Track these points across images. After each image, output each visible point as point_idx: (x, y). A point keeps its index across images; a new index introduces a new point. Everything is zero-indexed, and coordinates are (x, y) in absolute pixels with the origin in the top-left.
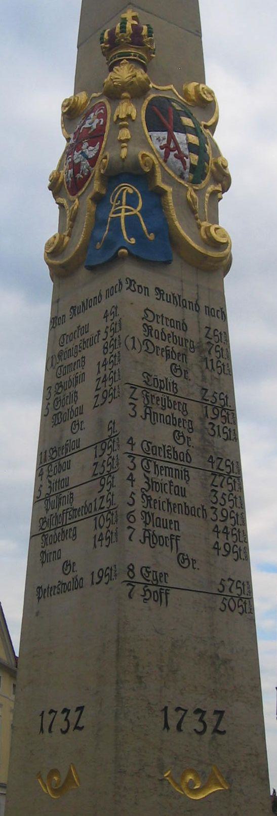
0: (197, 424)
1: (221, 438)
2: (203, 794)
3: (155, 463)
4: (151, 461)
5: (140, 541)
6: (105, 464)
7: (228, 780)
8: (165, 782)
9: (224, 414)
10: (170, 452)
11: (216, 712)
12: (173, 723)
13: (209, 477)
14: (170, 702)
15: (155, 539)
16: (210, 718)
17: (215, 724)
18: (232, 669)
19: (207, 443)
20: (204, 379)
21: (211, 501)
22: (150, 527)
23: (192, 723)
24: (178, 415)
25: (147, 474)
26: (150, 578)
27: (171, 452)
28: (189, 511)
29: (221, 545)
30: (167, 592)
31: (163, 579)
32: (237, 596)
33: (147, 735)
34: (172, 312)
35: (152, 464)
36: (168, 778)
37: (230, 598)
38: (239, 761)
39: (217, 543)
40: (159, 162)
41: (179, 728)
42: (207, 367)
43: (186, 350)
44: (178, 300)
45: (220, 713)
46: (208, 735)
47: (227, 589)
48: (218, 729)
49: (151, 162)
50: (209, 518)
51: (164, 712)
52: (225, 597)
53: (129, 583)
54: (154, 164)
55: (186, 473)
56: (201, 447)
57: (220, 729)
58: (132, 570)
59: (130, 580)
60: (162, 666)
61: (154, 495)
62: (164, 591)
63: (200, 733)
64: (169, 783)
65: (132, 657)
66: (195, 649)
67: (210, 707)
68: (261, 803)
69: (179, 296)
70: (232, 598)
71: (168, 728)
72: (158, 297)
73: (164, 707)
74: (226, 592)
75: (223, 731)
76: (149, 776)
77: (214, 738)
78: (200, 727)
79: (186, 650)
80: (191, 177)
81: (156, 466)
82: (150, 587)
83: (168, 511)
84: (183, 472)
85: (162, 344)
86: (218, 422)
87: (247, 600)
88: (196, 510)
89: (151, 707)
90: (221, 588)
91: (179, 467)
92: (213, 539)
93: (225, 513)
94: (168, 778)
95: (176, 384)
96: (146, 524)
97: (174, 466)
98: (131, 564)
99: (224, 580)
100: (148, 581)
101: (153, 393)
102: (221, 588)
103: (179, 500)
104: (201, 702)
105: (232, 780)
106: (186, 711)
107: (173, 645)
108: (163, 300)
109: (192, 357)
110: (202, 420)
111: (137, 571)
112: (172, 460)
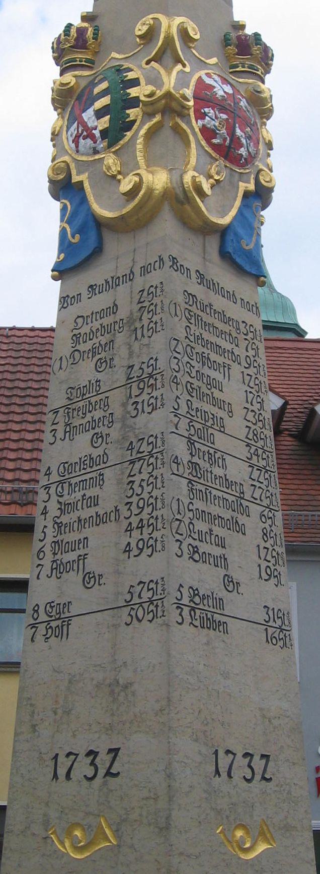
0: (118, 412)
1: (146, 414)
2: (89, 852)
3: (69, 482)
4: (65, 482)
5: (47, 575)
6: (144, 484)
7: (117, 832)
8: (49, 841)
9: (152, 381)
10: (85, 462)
11: (110, 751)
12: (62, 772)
13: (127, 468)
14: (61, 748)
15: (62, 566)
16: (103, 760)
18: (134, 694)
20: (131, 354)
21: (127, 496)
22: (58, 557)
23: (83, 768)
24: (98, 414)
25: (61, 500)
26: (54, 613)
27: (88, 462)
28: (100, 520)
29: (133, 545)
31: (66, 610)
32: (148, 600)
33: (35, 789)
34: (102, 301)
35: (66, 486)
36: (52, 836)
38: (133, 808)
39: (129, 544)
41: (68, 776)
42: (136, 338)
43: (114, 334)
44: (111, 285)
45: (114, 752)
46: (99, 780)
47: (136, 596)
48: (111, 771)
49: (63, 165)
50: (122, 517)
51: (54, 760)
52: (132, 606)
53: (33, 626)
54: (68, 165)
55: (101, 477)
56: (121, 438)
57: (113, 771)
58: (37, 611)
59: (35, 622)
60: (57, 709)
61: (65, 519)
62: (66, 623)
63: (90, 779)
64: (53, 841)
66: (92, 679)
68: (156, 860)
69: (112, 278)
70: (141, 606)
71: (57, 779)
72: (90, 296)
74: (136, 600)
76: (34, 834)
77: (105, 784)
81: (70, 485)
82: (53, 624)
83: (78, 530)
84: (98, 477)
85: (89, 345)
86: (145, 397)
87: (160, 602)
88: (108, 514)
90: (128, 597)
92: (125, 540)
93: (141, 504)
94: (52, 836)
95: (99, 381)
96: (55, 554)
98: (37, 605)
99: (133, 586)
101: (73, 406)
102: (128, 597)
103: (92, 511)
105: (122, 833)
106: (77, 755)
107: (70, 682)
108: (96, 294)
109: (120, 338)
110: (124, 405)
111: (41, 610)
112: (89, 470)
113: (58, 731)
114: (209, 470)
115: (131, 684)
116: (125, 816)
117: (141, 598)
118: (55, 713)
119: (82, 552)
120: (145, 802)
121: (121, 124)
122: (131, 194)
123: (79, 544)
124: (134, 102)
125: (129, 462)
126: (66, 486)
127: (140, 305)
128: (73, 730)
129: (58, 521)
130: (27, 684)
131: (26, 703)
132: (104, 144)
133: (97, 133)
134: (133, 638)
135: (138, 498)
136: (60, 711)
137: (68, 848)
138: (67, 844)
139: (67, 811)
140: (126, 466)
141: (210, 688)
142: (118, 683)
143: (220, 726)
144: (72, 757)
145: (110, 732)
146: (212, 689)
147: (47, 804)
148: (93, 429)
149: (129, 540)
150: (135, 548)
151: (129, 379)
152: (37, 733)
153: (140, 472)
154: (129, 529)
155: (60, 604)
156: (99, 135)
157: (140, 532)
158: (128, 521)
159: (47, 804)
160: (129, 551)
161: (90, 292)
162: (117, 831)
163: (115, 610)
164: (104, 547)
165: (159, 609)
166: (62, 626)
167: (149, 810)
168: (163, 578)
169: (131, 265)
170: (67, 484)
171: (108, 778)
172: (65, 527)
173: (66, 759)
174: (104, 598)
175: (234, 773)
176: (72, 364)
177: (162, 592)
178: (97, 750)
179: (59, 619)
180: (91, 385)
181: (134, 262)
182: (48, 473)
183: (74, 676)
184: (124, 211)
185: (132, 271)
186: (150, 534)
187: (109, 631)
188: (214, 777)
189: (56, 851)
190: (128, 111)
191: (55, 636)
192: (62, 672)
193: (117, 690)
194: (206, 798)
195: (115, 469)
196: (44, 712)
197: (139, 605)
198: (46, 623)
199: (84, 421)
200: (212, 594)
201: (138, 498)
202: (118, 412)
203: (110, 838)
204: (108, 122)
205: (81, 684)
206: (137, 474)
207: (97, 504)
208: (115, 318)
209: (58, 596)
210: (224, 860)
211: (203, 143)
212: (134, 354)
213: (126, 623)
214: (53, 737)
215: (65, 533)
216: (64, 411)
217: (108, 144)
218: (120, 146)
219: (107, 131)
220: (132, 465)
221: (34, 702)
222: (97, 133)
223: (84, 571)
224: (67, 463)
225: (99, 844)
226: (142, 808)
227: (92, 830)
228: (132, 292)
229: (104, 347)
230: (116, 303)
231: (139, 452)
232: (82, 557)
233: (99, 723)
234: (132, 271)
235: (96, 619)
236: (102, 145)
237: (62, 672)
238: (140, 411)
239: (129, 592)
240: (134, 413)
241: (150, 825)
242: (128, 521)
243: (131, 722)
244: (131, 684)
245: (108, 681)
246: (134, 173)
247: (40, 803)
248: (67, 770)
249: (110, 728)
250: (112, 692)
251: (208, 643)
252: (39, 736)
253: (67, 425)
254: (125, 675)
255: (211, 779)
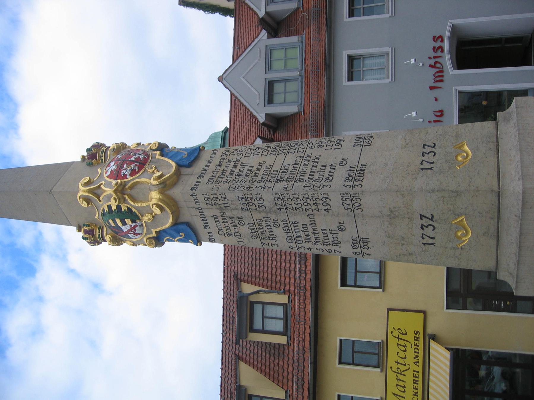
0: (263, 215)
3: (296, 238)
5: (339, 248)
6: (297, 203)
7: (459, 215)
8: (463, 247)
9: (249, 199)
10: (287, 230)
11: (421, 219)
12: (431, 241)
13: (289, 211)
15: (335, 241)
16: (425, 222)
17: (428, 220)
18: (394, 208)
19: (271, 211)
20: (236, 209)
21: (302, 211)
22: (331, 243)
23: (429, 231)
24: (264, 224)
25: (304, 242)
26: (357, 245)
27: (286, 229)
28: (313, 223)
29: (325, 208)
30: (361, 238)
31: (355, 239)
32: (351, 201)
34: (211, 222)
35: (297, 239)
36: (461, 246)
37: (354, 207)
38: (448, 208)
39: (324, 210)
40: (144, 236)
41: (433, 238)
42: (229, 206)
43: (227, 217)
45: (422, 217)
47: (349, 207)
48: (431, 218)
49: (148, 241)
50: (312, 213)
51: (425, 245)
52: (354, 208)
53: (363, 255)
54: (148, 238)
55: (293, 223)
56: (275, 213)
57: (430, 217)
58: (356, 253)
61: (313, 240)
62: (361, 239)
64: (463, 245)
65: (400, 257)
66: (388, 227)
67: (420, 222)
68: (472, 197)
69: (200, 218)
70: (353, 204)
71: (434, 243)
72: (209, 228)
73: (423, 245)
74: (351, 207)
75: (431, 216)
77: (436, 221)
78: (432, 228)
79: (390, 231)
80: (138, 221)
81: (297, 237)
82: (362, 245)
83: (318, 234)
84: (294, 224)
85: (232, 229)
86: (256, 202)
87: (352, 195)
89: (424, 250)
90: (349, 210)
91: (292, 226)
94: (461, 246)
95: (249, 224)
96: (329, 244)
97: (293, 229)
98: (353, 253)
99: (344, 208)
100: (358, 246)
101: (260, 236)
102: (349, 210)
103: (309, 227)
104: (417, 226)
105: (459, 213)
106: (423, 234)
107: (389, 237)
108: (208, 225)
109: (229, 214)
110: (260, 212)
111: (356, 251)
112: (290, 229)
113: (412, 243)
114: (290, 172)
115: (390, 209)
116: (452, 212)
117: (350, 204)
118: (404, 244)
119: (328, 232)
120: (445, 203)
121: (129, 213)
122: (161, 209)
123: (324, 233)
124: (119, 207)
125: (287, 210)
126: (297, 239)
127: (213, 205)
128: (411, 236)
129: (314, 243)
130: (390, 257)
131: (399, 258)
132: (138, 221)
133: (133, 225)
134: (368, 208)
135: (303, 205)
136: (403, 242)
137: (467, 238)
138: (465, 239)
139: (449, 239)
140: (288, 211)
141: (392, 172)
142: (389, 215)
143: (409, 167)
144: (424, 236)
145: (412, 219)
146: (392, 171)
147: (446, 248)
148: (271, 226)
149: (323, 210)
150: (327, 207)
151: (248, 210)
152: (413, 253)
153: (291, 205)
154: (317, 210)
155: (353, 242)
156: (134, 224)
157: (319, 205)
158: (314, 210)
159: (446, 248)
160: (328, 210)
161: (207, 228)
162: (458, 215)
163: (355, 216)
164: (326, 221)
165: (355, 196)
166: (363, 241)
167: (449, 201)
168: (341, 194)
169: (194, 209)
170: (297, 239)
171: (434, 220)
172: (317, 240)
173: (425, 239)
174: (350, 221)
175: (432, 161)
176: (241, 236)
177: (347, 194)
178: (421, 225)
179: (359, 242)
180: (251, 227)
181: (193, 207)
182: (291, 248)
183: (386, 235)
184: (169, 212)
185: (198, 209)
186: (320, 200)
187: (365, 219)
188: (433, 170)
189: (468, 244)
190: (123, 211)
191: (368, 244)
192: (384, 241)
193: (393, 216)
194: (443, 174)
195: (290, 216)
196: (403, 249)
197: (353, 205)
198: (362, 248)
199: (267, 231)
200: (348, 171)
201: (303, 205)
202: (263, 215)
203: (462, 218)
204: (128, 220)
205: (390, 232)
206: (292, 206)
207: (306, 224)
208: (219, 217)
209: (349, 243)
210: (472, 166)
211: (138, 175)
212: (236, 207)
213: (362, 211)
214: (414, 245)
215: (319, 240)
216: (263, 240)
217: (138, 219)
218: (139, 214)
219: (132, 220)
220: (288, 208)
221: (399, 254)
222: (133, 225)
223: (337, 231)
224: (287, 239)
225: (465, 224)
226: (447, 203)
227: (458, 227)
228: (207, 209)
229: (233, 222)
230: (212, 216)
231: (282, 205)
232: (331, 232)
233: (408, 224)
234: (198, 209)
235: (360, 225)
236: (139, 223)
237: (384, 241)
238: (262, 205)
239: (347, 210)
240: (264, 207)
241: (455, 200)
242: (314, 210)
243: (408, 209)
244: (390, 209)
245: (389, 220)
246: (152, 207)
247: (446, 252)
248: (430, 239)
249: (411, 219)
250: (394, 218)
251: (371, 173)
252: (414, 252)
253: (269, 239)
254: (386, 212)
255: (434, 172)
